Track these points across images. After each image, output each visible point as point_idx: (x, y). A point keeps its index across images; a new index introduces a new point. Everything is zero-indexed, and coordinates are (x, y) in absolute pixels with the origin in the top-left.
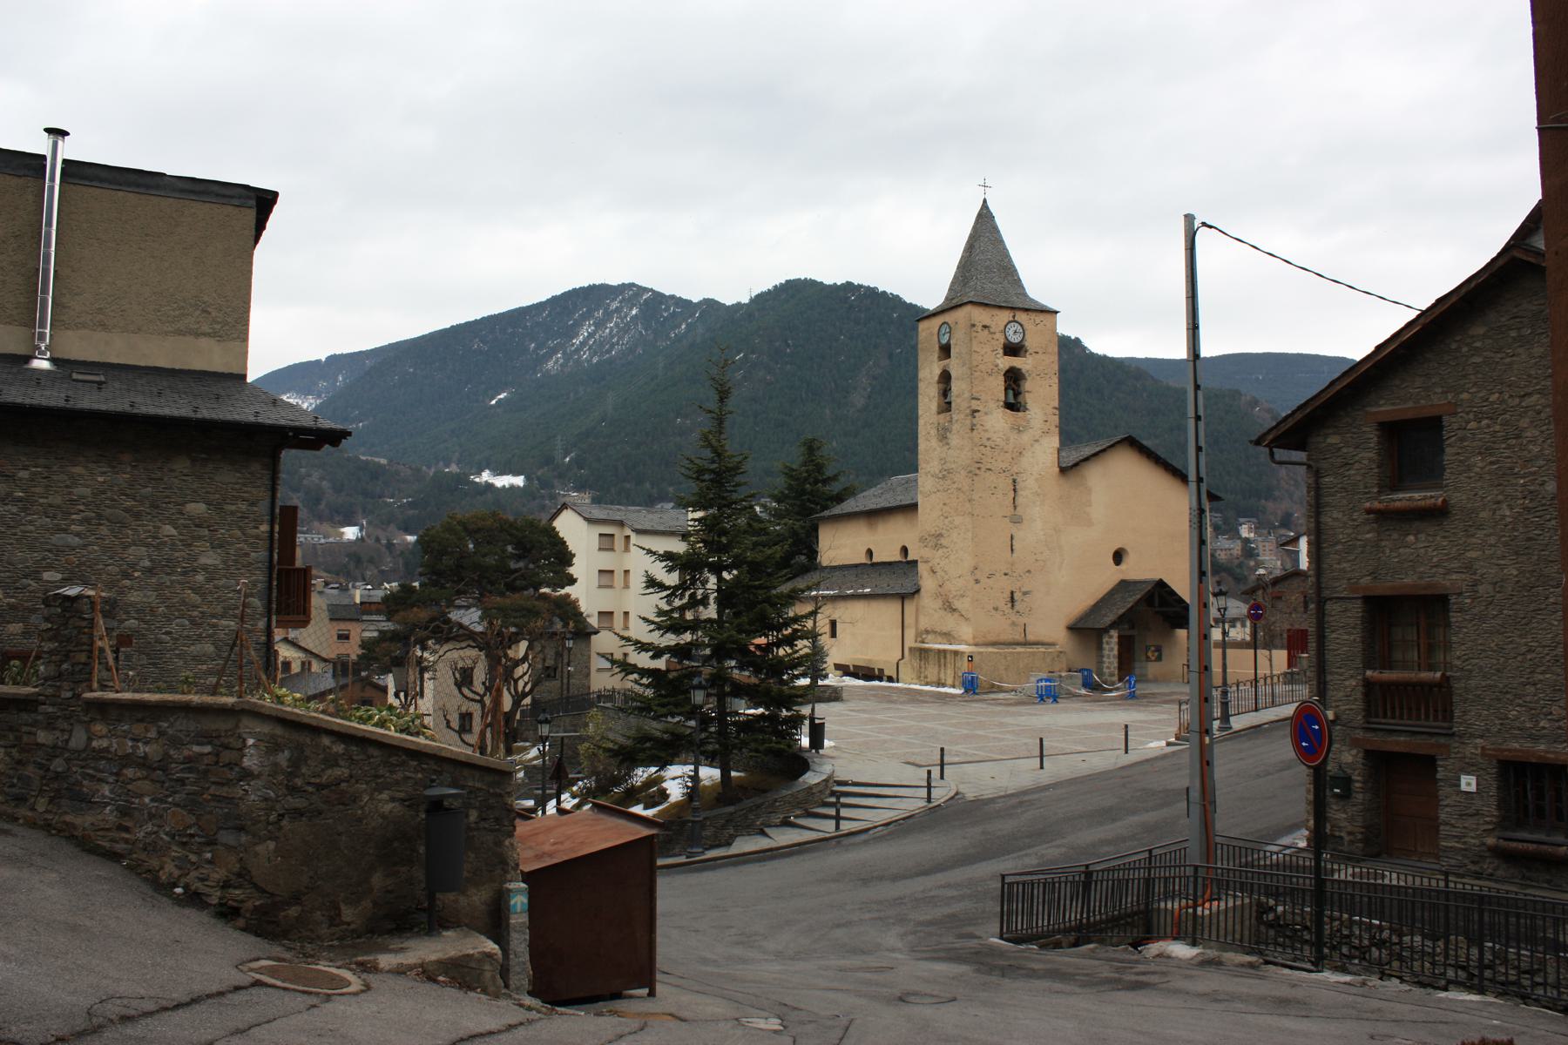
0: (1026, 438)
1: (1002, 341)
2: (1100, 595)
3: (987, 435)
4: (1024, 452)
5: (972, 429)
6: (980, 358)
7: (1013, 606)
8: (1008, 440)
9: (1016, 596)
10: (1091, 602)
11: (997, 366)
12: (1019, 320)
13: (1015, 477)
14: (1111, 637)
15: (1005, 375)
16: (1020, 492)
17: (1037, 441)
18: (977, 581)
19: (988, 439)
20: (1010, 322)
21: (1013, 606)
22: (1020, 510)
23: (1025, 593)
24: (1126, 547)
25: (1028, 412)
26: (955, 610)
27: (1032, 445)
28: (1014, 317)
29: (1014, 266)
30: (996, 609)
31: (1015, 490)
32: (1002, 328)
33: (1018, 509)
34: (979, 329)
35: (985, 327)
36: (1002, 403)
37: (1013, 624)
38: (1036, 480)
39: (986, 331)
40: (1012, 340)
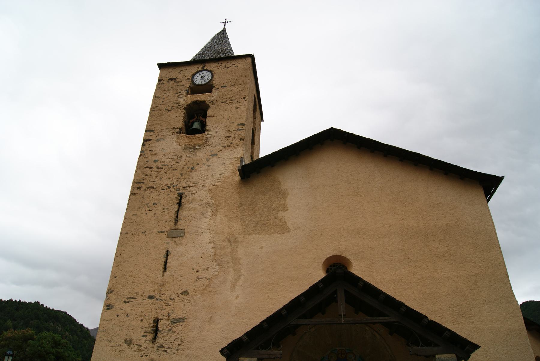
0: (200, 154)
3: (154, 158)
4: (197, 167)
7: (154, 339)
8: (179, 158)
12: (209, 68)
13: (181, 191)
16: (185, 205)
17: (216, 155)
19: (155, 161)
21: (154, 339)
22: (182, 224)
23: (175, 321)
25: (206, 133)
27: (207, 160)
30: (129, 342)
31: (180, 204)
33: (179, 223)
35: (171, 79)
38: (210, 191)
39: (172, 82)
40: (200, 83)
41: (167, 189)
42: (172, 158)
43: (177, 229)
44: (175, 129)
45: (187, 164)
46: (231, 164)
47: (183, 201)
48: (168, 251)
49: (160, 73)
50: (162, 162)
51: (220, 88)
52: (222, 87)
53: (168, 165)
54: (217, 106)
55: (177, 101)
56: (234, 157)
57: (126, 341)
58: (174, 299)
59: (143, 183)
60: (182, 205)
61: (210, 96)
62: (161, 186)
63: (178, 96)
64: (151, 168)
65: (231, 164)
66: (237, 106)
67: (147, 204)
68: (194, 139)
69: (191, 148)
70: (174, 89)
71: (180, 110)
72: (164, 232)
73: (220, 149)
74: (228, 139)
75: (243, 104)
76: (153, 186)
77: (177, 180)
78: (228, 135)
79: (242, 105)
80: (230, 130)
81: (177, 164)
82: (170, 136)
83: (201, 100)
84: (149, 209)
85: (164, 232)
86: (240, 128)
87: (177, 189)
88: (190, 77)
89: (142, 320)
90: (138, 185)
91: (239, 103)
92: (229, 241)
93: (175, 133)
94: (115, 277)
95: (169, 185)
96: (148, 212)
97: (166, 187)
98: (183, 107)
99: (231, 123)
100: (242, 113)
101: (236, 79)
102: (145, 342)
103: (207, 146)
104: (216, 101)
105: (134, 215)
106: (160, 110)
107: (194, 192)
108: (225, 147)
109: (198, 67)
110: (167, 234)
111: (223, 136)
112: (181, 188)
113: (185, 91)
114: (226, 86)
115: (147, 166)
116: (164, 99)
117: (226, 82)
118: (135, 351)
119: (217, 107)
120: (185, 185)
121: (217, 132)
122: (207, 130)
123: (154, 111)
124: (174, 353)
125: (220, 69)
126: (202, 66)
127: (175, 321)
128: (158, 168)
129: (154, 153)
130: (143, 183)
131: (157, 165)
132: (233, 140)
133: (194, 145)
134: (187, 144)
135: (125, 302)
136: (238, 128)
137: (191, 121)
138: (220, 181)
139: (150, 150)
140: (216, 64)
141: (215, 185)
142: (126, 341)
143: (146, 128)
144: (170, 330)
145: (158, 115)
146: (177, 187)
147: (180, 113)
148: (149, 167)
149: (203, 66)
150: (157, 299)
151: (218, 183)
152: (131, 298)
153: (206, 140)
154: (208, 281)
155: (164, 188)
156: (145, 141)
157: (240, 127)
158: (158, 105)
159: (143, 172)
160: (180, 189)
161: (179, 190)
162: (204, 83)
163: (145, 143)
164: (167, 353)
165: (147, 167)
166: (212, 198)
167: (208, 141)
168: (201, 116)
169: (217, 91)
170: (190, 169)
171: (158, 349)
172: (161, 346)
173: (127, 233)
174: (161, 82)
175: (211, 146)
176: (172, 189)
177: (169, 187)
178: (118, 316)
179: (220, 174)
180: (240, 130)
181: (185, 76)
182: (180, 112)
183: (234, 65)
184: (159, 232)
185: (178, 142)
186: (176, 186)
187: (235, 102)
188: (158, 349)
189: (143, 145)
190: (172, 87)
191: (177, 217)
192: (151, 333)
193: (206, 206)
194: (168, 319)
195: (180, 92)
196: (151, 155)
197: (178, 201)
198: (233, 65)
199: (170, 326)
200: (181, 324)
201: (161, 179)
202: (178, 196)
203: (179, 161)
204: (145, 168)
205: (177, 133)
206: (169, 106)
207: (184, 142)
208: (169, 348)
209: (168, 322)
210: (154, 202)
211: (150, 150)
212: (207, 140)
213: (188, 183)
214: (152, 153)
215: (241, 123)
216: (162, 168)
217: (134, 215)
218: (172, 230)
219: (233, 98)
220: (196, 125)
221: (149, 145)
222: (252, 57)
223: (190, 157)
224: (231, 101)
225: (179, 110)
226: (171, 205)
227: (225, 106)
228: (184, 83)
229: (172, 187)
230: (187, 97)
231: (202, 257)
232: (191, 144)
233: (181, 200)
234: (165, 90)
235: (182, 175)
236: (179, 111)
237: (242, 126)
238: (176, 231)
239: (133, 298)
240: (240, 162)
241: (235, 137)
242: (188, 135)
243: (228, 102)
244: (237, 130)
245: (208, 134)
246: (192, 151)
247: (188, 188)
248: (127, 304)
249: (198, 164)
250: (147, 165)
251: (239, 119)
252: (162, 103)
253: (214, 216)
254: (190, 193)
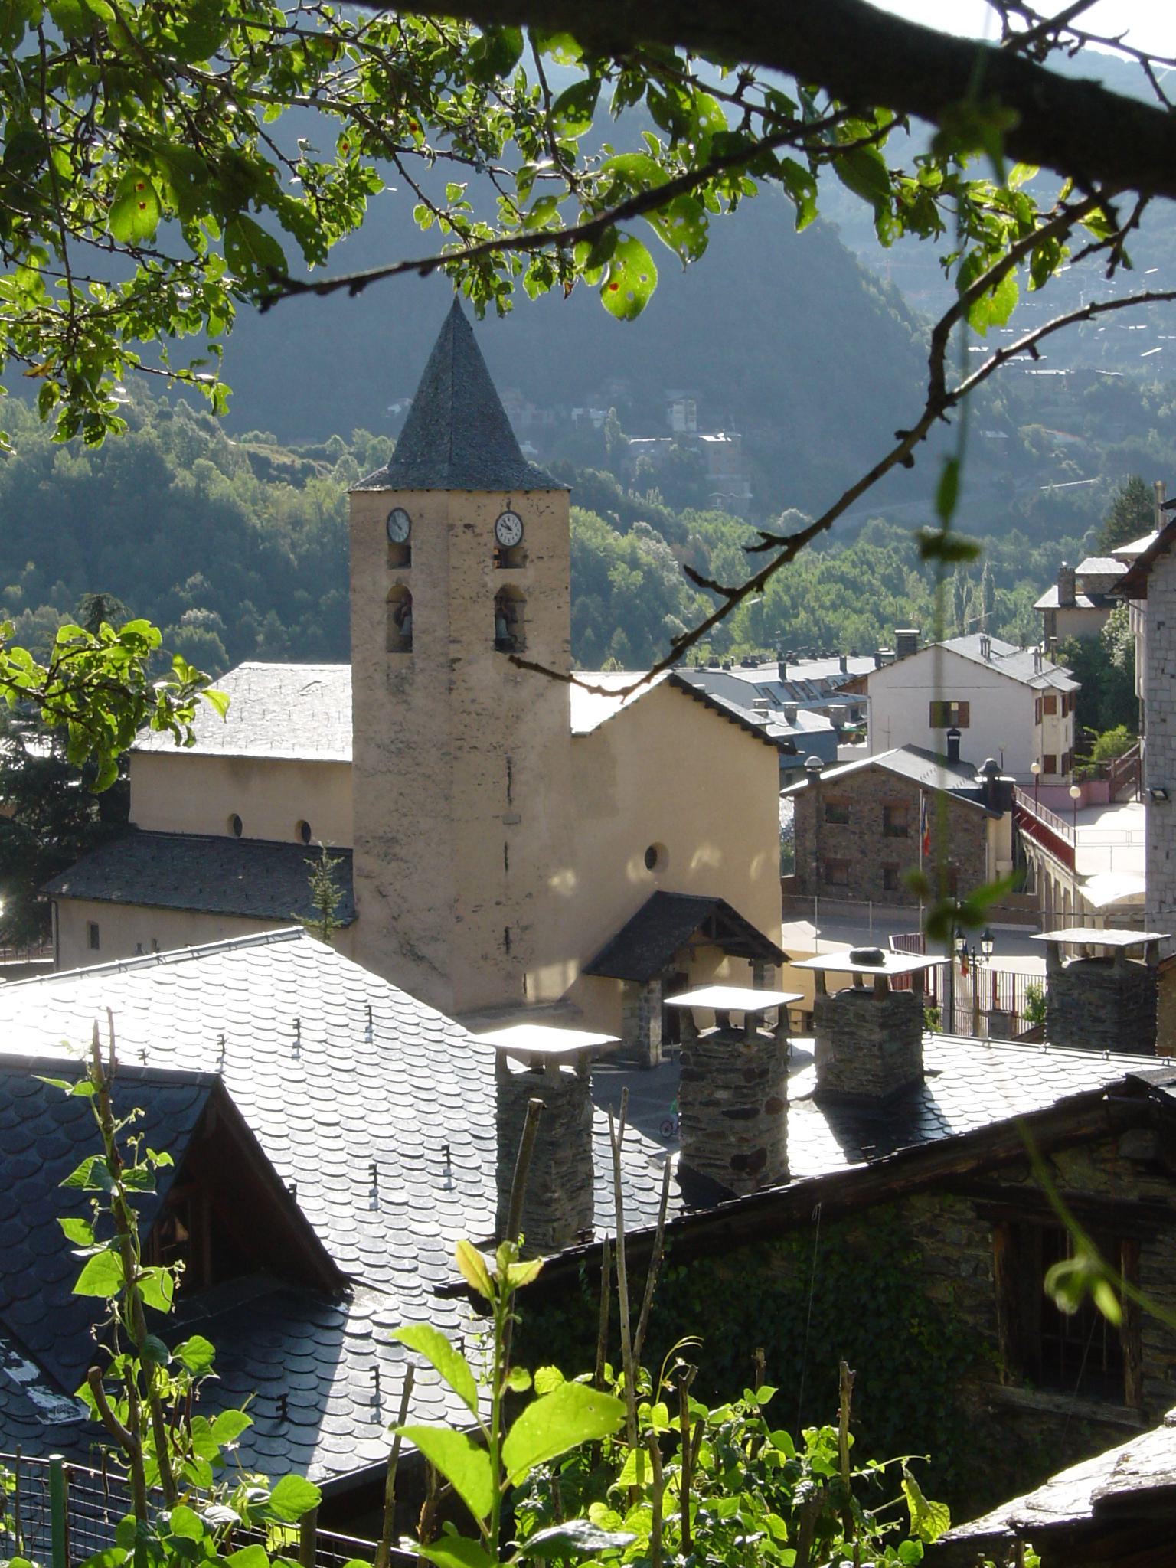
2: (628, 917)
5: (451, 689)
7: (508, 949)
10: (616, 928)
11: (484, 586)
12: (516, 511)
13: (510, 754)
14: (651, 991)
18: (459, 919)
19: (473, 701)
21: (508, 949)
23: (525, 928)
26: (422, 958)
28: (508, 505)
31: (509, 775)
32: (492, 526)
33: (515, 803)
34: (460, 530)
35: (468, 526)
36: (492, 643)
39: (469, 533)
105: (463, 792)
127: (525, 928)
165: (464, 712)
233: (509, 768)
235: (507, 727)
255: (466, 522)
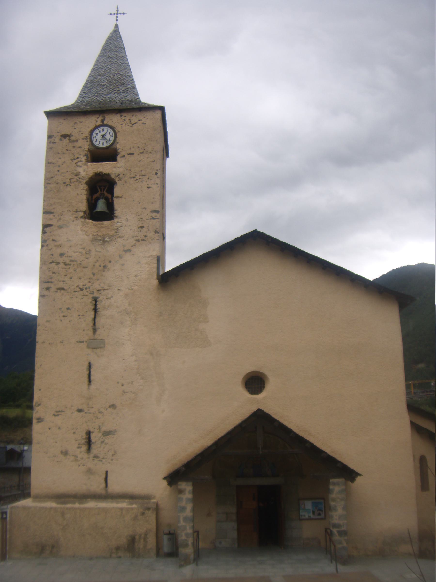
1: (86, 146)
3: (60, 251)
4: (109, 266)
6: (57, 169)
7: (89, 449)
8: (88, 253)
9: (93, 437)
10: (208, 442)
11: (77, 174)
12: (110, 123)
13: (96, 295)
15: (87, 183)
16: (101, 312)
17: (128, 251)
19: (62, 255)
20: (96, 127)
21: (89, 449)
23: (107, 433)
24: (265, 371)
25: (116, 220)
27: (121, 257)
29: (131, 76)
30: (65, 453)
31: (95, 310)
33: (98, 332)
35: (65, 136)
36: (82, 214)
37: (89, 471)
38: (126, 296)
39: (66, 141)
40: (101, 145)
41: (79, 292)
42: (79, 252)
43: (96, 339)
44: (78, 213)
45: (97, 261)
46: (147, 263)
47: (98, 306)
48: (90, 363)
49: (50, 124)
50: (70, 256)
51: (126, 155)
52: (128, 154)
53: (76, 261)
54: (125, 183)
55: (76, 170)
56: (149, 255)
57: (62, 452)
58: (102, 413)
59: (52, 282)
60: (98, 311)
61: (115, 167)
62: (73, 287)
63: (76, 163)
64: (58, 263)
65: (147, 263)
66: (148, 185)
67: (60, 309)
68: (101, 227)
69: (101, 240)
70: (70, 151)
71: (82, 184)
72: (83, 342)
73: (133, 244)
74: (141, 231)
75: (156, 183)
76: (63, 287)
77: (89, 280)
78: (141, 225)
79: (154, 184)
80: (142, 218)
81: (86, 260)
82: (73, 221)
83: (105, 173)
84: (62, 315)
85: (83, 342)
86: (153, 217)
87: (91, 292)
88: (87, 135)
89: (74, 433)
90: (46, 285)
91: (151, 180)
92: (151, 354)
93: (79, 218)
94: (40, 390)
95: (81, 287)
96: (63, 318)
97: (78, 289)
98: (85, 181)
99: (143, 209)
100: (155, 195)
101: (145, 144)
102: (81, 452)
103: (118, 238)
104: (124, 174)
105: (47, 321)
106: (57, 183)
107: (109, 296)
108: (138, 241)
109: (96, 119)
110: (86, 344)
111: (135, 226)
112: (95, 291)
113: (84, 156)
114: (133, 154)
115: (52, 261)
116: (59, 166)
117: (133, 147)
118: (72, 461)
119: (125, 184)
120: (99, 288)
121: (127, 220)
122: (117, 217)
123: (50, 184)
124: (109, 463)
125: (124, 125)
126: (101, 118)
127: (107, 433)
128: (66, 264)
129: (58, 243)
130: (52, 282)
131: (64, 261)
132: (146, 232)
133: (104, 237)
134: (95, 234)
135: (55, 415)
136: (151, 216)
137: (95, 197)
138: (137, 284)
139: (53, 240)
140: (119, 115)
141: (132, 289)
142: (62, 452)
143: (44, 209)
144: (103, 442)
145: (55, 190)
146: (91, 288)
147: (82, 190)
148: (55, 262)
149: (102, 118)
150: (86, 413)
151: (134, 286)
152: (59, 411)
153: (116, 230)
154: (134, 395)
155: (75, 290)
156: (45, 226)
157: (154, 215)
158: (53, 175)
159: (49, 269)
160: (93, 292)
161: (92, 293)
162: (106, 145)
163: (45, 229)
164: (103, 463)
165: (53, 262)
166: (130, 304)
167: (118, 231)
168: (105, 190)
169: (123, 160)
170: (102, 268)
171: (93, 459)
172: (96, 457)
173: (43, 343)
174: (52, 140)
175: (123, 238)
176: (84, 291)
177: (82, 289)
178: (50, 429)
179: (136, 276)
180: (154, 219)
181: (81, 133)
182: (82, 189)
183: (141, 120)
184: (77, 342)
185: (84, 231)
186: (89, 288)
187: (145, 178)
188: (93, 459)
189: (44, 232)
190: (66, 149)
191: (94, 324)
192: (85, 445)
193: (125, 314)
194: (99, 432)
195: (78, 158)
196: (55, 246)
197: (93, 307)
198: (139, 120)
199: (102, 439)
200: (113, 436)
201: (71, 278)
202: (93, 300)
203: (88, 256)
204: (51, 263)
205: (82, 217)
206: (67, 178)
207: (92, 231)
208: (104, 458)
209: (100, 435)
210: (67, 307)
211: (53, 240)
212: (117, 230)
213: (102, 285)
214: (56, 244)
215: (155, 209)
216: (70, 265)
217: (47, 321)
218: (92, 340)
219: (143, 173)
220: (101, 206)
221: (51, 232)
222: (162, 109)
223: (100, 252)
224: (141, 177)
225: (80, 184)
226: (87, 311)
227: (134, 183)
228: (81, 143)
229: (84, 289)
230: (87, 166)
231: (125, 371)
232: (99, 234)
233: (96, 305)
234: (58, 153)
235: (94, 274)
236: (80, 186)
237: (156, 214)
238: (95, 341)
239: (62, 411)
240: (156, 262)
241: (148, 228)
242: (94, 222)
243: (137, 177)
244: (151, 219)
245: (118, 222)
246: (102, 244)
247: (102, 291)
248: (57, 417)
249: (110, 262)
250: (52, 259)
251: (152, 203)
252: (57, 173)
253: (133, 326)
254: (105, 297)
255: (63, 133)
